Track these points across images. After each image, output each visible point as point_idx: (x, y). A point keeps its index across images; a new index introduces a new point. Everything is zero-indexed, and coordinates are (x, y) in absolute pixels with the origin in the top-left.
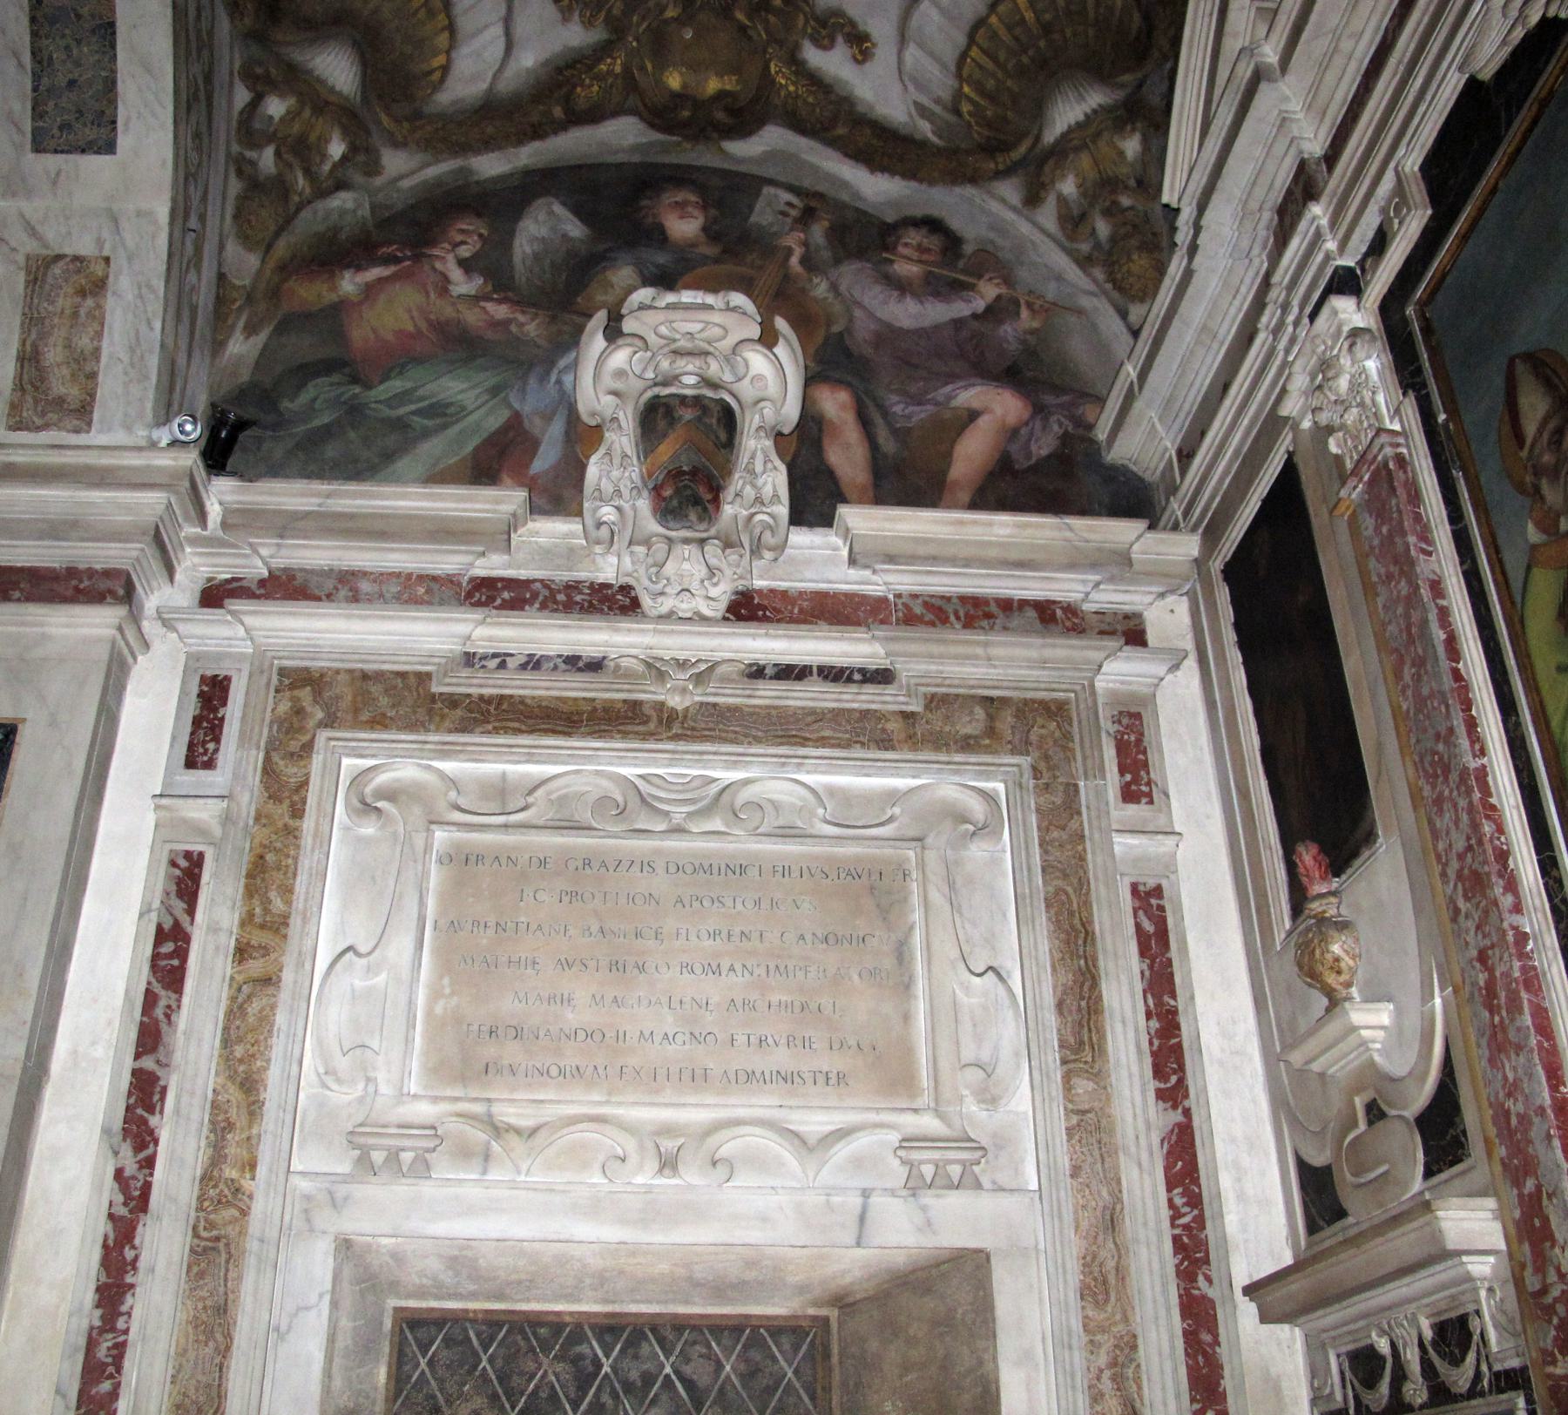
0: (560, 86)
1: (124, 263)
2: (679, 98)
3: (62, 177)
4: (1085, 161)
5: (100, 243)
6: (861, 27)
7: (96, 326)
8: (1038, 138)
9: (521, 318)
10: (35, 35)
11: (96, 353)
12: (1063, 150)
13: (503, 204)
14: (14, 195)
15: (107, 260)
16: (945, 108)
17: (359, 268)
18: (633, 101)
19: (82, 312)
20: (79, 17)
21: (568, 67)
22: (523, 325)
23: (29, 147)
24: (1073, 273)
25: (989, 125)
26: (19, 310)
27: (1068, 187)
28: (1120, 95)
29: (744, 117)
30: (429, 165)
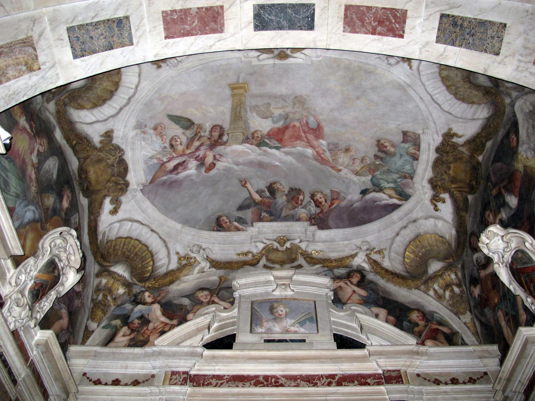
0: (81, 140)
1: (40, 76)
2: (86, 172)
3: (61, 42)
4: (112, 281)
5: (44, 64)
6: (119, 210)
7: (17, 75)
8: (111, 266)
9: (34, 184)
10: (104, 21)
11: (9, 80)
12: (112, 274)
13: (55, 150)
14: (51, 24)
15: (40, 69)
16: (107, 239)
17: (26, 120)
18: (82, 160)
19: (20, 67)
20: (112, 36)
21: (87, 141)
22: (33, 185)
23: (68, 26)
24: (90, 300)
25: (108, 252)
26: (12, 40)
27: (104, 281)
28: (130, 280)
29: (88, 192)
30: (53, 115)
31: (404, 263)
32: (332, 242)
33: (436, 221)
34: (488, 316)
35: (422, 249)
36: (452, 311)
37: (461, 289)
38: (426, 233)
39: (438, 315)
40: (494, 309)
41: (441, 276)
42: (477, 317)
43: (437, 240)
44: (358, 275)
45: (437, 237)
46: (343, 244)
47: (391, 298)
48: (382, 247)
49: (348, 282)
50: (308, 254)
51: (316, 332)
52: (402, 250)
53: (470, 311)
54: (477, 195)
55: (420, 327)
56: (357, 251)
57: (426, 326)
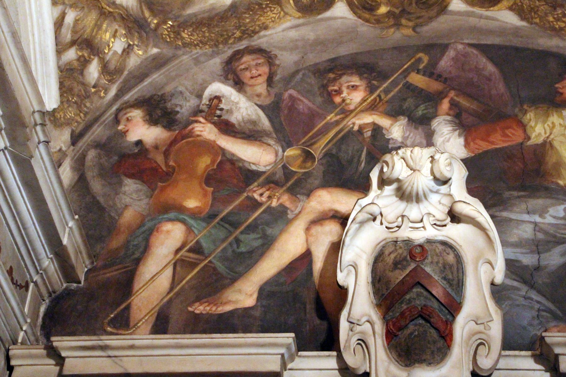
37: (104, 81)
40: (167, 210)
41: (104, 14)
53: (75, 139)
54: (365, 29)
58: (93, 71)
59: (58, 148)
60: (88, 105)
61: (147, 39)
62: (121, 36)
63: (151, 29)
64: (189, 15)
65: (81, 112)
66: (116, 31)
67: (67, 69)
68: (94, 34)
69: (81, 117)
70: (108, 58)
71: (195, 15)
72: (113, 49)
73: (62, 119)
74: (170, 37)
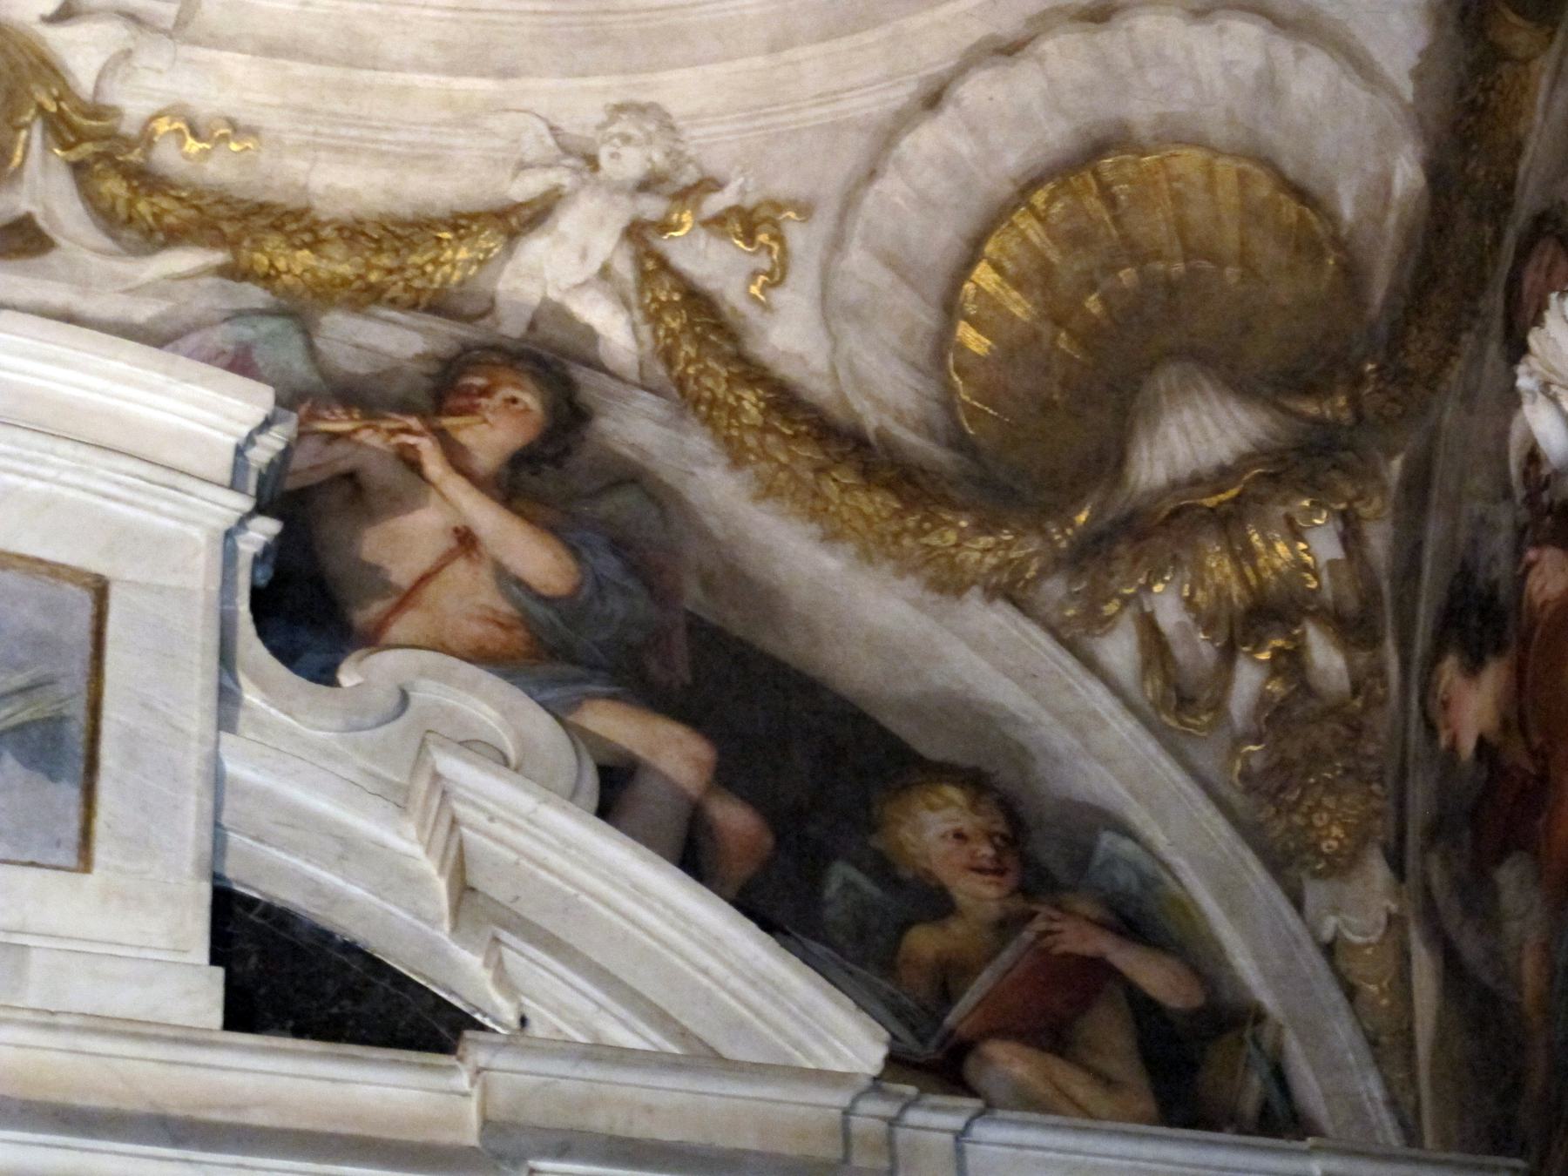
31: (939, 357)
32: (351, 63)
33: (1284, 49)
34: (1513, 927)
35: (1111, 269)
36: (1250, 833)
37: (1362, 658)
38: (1175, 135)
39: (1127, 847)
41: (1228, 521)
42: (1430, 912)
43: (1252, 214)
44: (529, 399)
45: (1263, 189)
46: (449, 102)
47: (768, 641)
48: (783, 185)
49: (427, 448)
50: (111, 135)
51: (68, 857)
52: (940, 239)
53: (1397, 865)
55: (957, 927)
56: (561, 177)
57: (1006, 927)
58: (1326, 658)
59: (1383, 919)
60: (1371, 749)
61: (1361, 459)
62: (1309, 518)
63: (1351, 429)
64: (1387, 305)
65: (1369, 783)
66: (1290, 520)
67: (1268, 721)
68: (1253, 582)
69: (1378, 797)
70: (1328, 595)
71: (1394, 289)
72: (1322, 561)
73: (1346, 842)
74: (1394, 400)
